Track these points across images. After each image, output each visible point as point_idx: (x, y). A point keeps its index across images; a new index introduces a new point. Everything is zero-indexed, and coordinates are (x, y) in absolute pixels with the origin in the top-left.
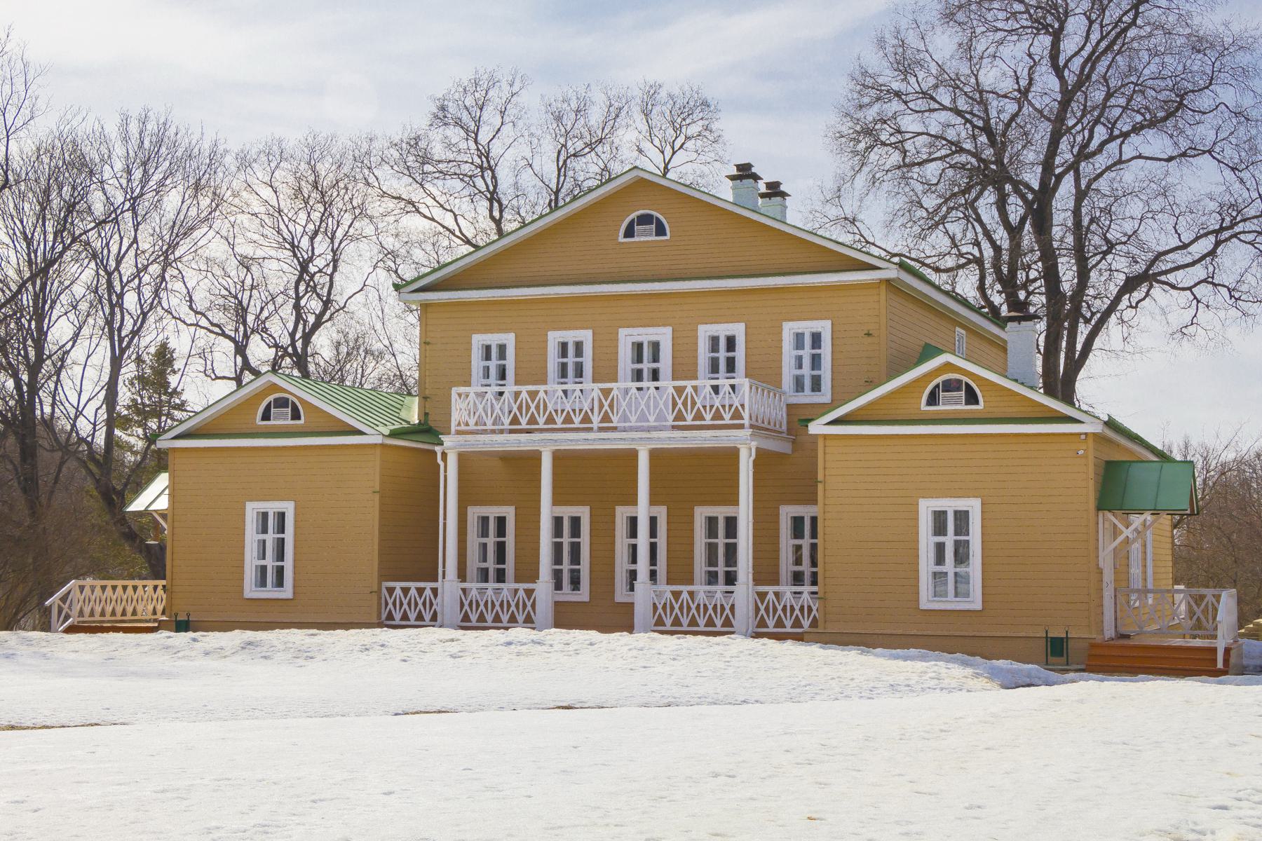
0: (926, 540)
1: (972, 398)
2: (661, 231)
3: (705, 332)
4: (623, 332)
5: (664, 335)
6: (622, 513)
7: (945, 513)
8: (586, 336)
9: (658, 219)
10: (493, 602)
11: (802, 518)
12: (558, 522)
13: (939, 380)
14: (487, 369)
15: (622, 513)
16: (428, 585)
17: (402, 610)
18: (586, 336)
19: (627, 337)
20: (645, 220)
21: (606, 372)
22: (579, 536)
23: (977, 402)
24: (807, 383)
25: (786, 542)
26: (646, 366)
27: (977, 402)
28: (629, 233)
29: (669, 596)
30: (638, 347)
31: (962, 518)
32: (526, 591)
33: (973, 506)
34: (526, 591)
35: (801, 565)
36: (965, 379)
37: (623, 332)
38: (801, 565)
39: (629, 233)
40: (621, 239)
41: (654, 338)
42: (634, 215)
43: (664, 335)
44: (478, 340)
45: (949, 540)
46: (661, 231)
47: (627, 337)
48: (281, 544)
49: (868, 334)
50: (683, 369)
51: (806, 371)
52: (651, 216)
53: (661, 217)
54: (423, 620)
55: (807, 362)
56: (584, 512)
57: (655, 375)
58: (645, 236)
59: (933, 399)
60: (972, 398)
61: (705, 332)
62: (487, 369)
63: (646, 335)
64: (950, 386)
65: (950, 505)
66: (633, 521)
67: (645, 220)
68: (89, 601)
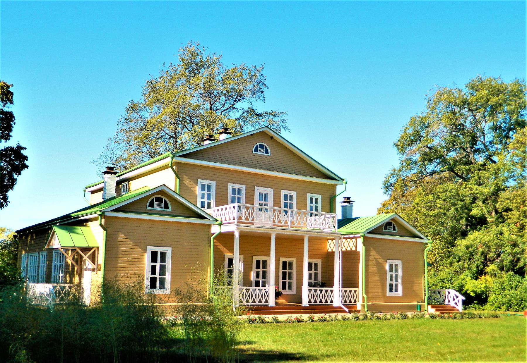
2: (267, 152)
5: (270, 192)
11: (259, 261)
12: (310, 265)
16: (353, 289)
17: (314, 299)
20: (262, 146)
28: (256, 150)
29: (244, 290)
32: (246, 289)
34: (246, 289)
35: (155, 274)
38: (155, 274)
39: (256, 150)
41: (266, 192)
42: (258, 144)
43: (270, 192)
45: (158, 265)
46: (267, 152)
48: (397, 276)
51: (205, 200)
58: (261, 153)
63: (264, 190)
68: (354, 297)
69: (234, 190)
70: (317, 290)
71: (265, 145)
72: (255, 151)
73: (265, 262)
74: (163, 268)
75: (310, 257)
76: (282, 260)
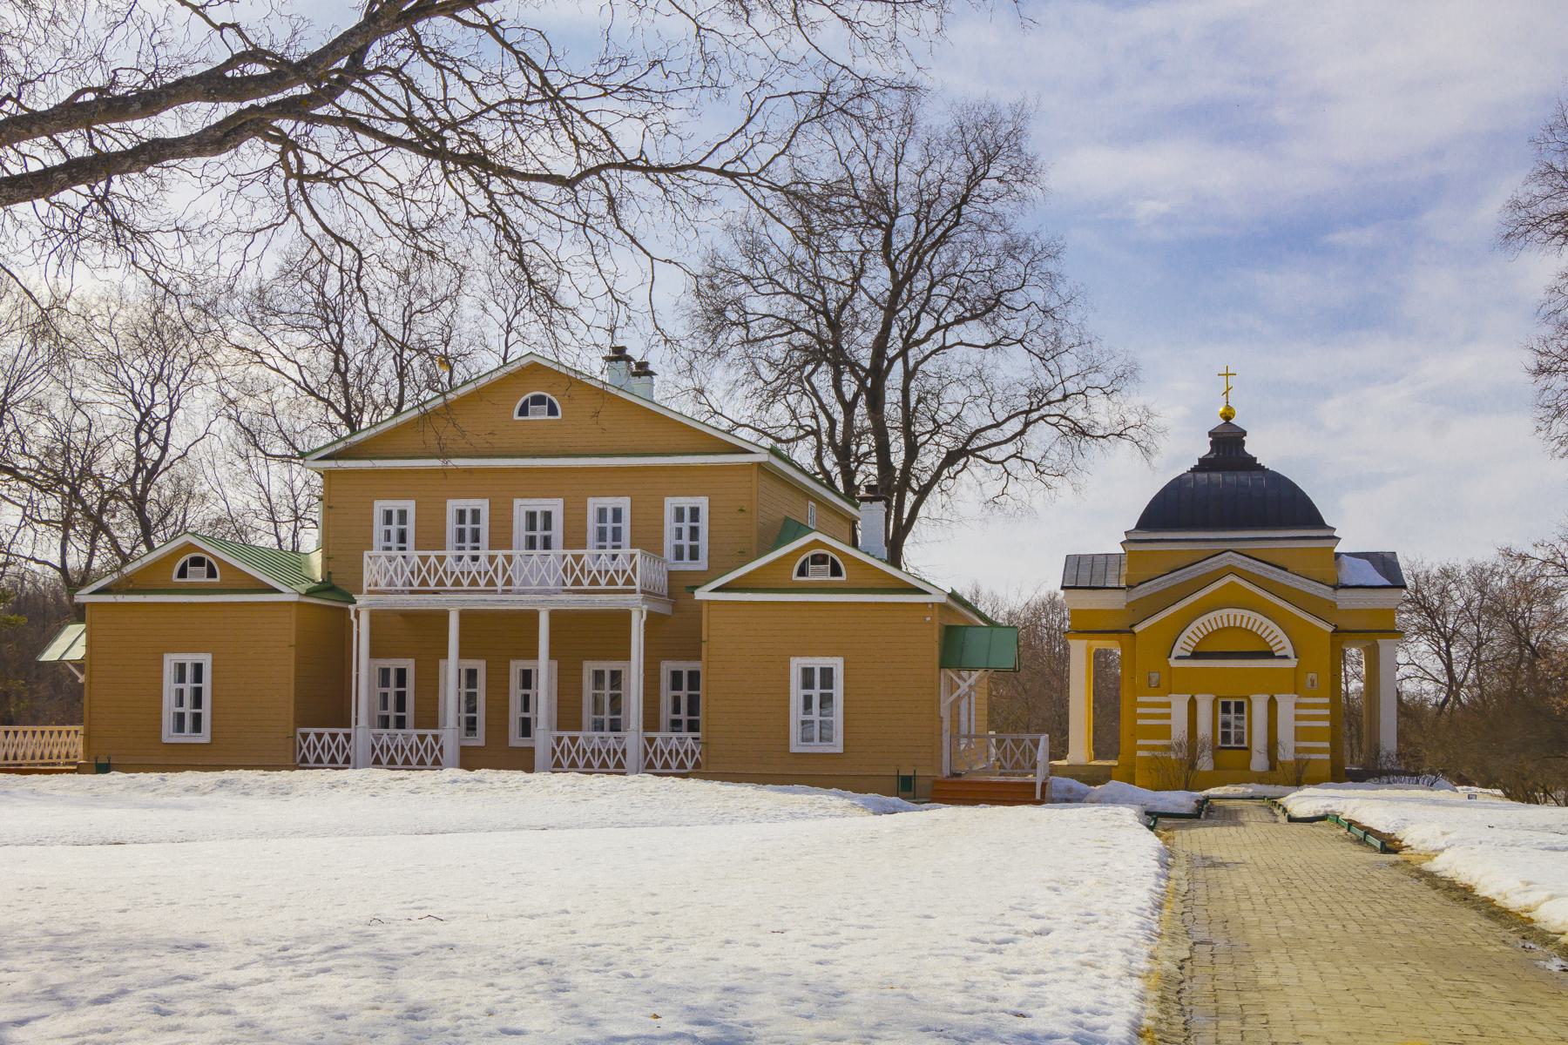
0: (796, 693)
1: (836, 571)
3: (593, 504)
4: (517, 502)
5: (556, 506)
6: (516, 667)
7: (812, 669)
8: (483, 505)
9: (550, 400)
10: (388, 746)
13: (809, 554)
14: (388, 533)
15: (516, 667)
18: (483, 505)
19: (521, 507)
20: (538, 400)
21: (501, 539)
22: (475, 687)
23: (840, 574)
24: (687, 552)
25: (666, 695)
26: (539, 533)
27: (840, 574)
28: (523, 411)
30: (532, 516)
31: (827, 674)
33: (837, 664)
35: (679, 713)
36: (831, 554)
37: (517, 502)
38: (679, 713)
39: (523, 411)
40: (516, 417)
42: (528, 396)
43: (556, 506)
44: (380, 506)
46: (553, 411)
47: (521, 507)
49: (741, 510)
50: (574, 539)
51: (686, 542)
52: (544, 397)
53: (556, 402)
54: (322, 762)
55: (686, 533)
56: (480, 666)
57: (547, 544)
58: (539, 415)
59: (802, 572)
60: (836, 571)
61: (593, 504)
62: (388, 533)
63: (539, 505)
64: (819, 560)
65: (818, 663)
66: (527, 678)
67: (538, 400)
69: (679, 514)
70: (337, 735)
71: (548, 395)
72: (557, 414)
73: (616, 675)
74: (826, 700)
75: (463, 655)
76: (667, 667)
